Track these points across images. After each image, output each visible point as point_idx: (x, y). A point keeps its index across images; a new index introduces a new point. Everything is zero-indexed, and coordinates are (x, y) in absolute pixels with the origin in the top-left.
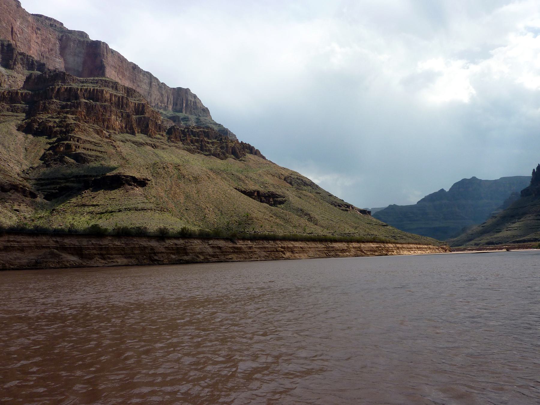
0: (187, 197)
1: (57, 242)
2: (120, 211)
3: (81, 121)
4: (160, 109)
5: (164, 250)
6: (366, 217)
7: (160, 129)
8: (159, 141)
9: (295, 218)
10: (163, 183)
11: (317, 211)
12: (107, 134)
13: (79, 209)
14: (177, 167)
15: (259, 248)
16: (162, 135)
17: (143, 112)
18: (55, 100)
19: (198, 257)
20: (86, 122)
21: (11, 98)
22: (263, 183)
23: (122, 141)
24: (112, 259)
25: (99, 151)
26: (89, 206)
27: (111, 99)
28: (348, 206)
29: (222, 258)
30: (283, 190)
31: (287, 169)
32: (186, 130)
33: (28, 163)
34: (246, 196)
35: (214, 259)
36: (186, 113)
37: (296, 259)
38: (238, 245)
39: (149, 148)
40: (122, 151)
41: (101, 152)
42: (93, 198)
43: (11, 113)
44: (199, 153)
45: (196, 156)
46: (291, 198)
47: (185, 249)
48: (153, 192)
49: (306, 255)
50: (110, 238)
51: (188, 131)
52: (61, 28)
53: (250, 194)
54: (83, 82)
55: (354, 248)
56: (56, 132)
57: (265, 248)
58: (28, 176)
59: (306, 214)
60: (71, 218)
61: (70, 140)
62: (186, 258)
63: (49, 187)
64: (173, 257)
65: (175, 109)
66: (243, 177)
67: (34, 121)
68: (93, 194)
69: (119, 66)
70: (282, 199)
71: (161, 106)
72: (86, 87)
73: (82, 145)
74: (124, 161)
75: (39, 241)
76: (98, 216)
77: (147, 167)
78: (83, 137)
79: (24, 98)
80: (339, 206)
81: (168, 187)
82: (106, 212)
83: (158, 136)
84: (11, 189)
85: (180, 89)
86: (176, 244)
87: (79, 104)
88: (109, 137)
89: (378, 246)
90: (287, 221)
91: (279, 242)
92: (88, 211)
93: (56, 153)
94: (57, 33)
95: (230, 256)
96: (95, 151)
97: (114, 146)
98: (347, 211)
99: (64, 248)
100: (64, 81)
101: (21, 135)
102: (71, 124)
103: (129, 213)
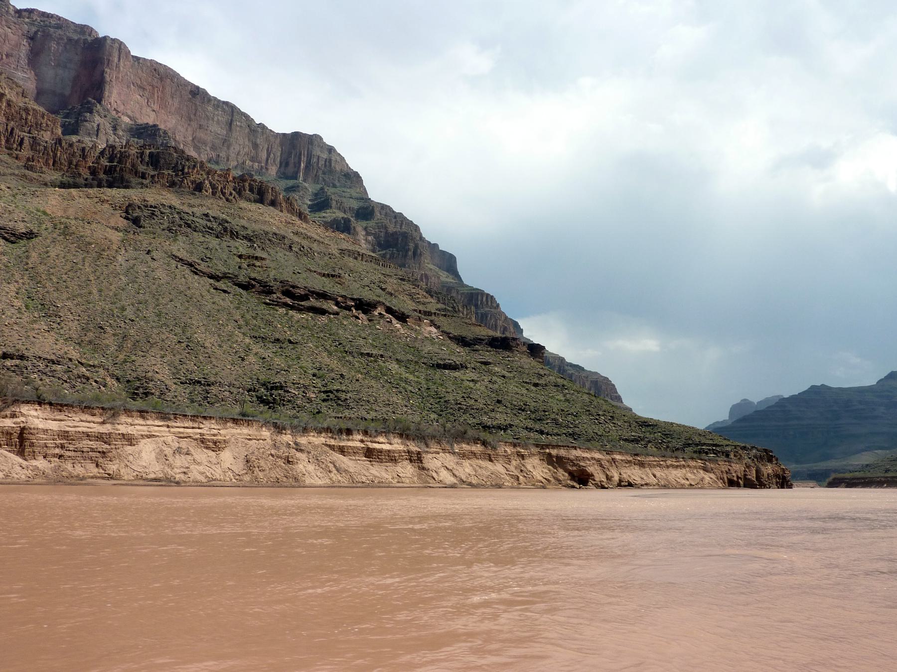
36: (305, 180)
65: (284, 173)
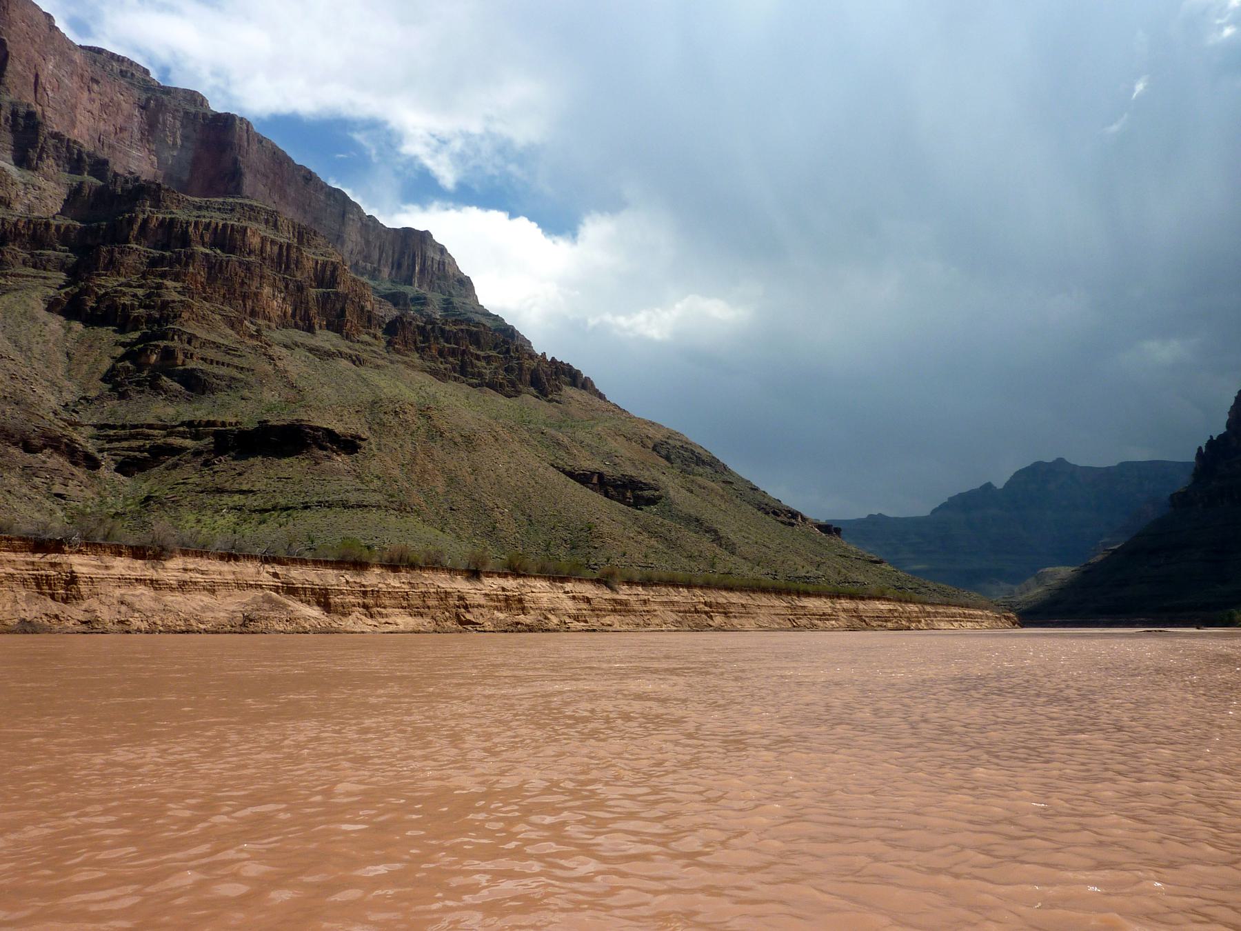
0: (452, 481)
1: (275, 575)
3: (196, 296)
4: (362, 274)
5: (483, 601)
6: (834, 540)
7: (369, 321)
8: (368, 348)
9: (690, 538)
10: (397, 446)
11: (732, 522)
12: (253, 328)
13: (208, 500)
14: (424, 412)
15: (662, 603)
16: (375, 337)
17: (333, 282)
18: (135, 246)
19: (546, 618)
20: (205, 299)
22: (609, 455)
23: (286, 346)
24: (387, 616)
25: (237, 367)
26: (232, 492)
27: (262, 250)
28: (794, 515)
29: (593, 621)
30: (656, 473)
31: (660, 426)
33: (74, 388)
34: (578, 485)
35: (580, 625)
36: (420, 286)
37: (734, 630)
38: (621, 597)
39: (344, 363)
40: (288, 369)
41: (242, 368)
42: (240, 474)
43: (31, 271)
44: (456, 379)
45: (451, 386)
46: (672, 493)
47: (520, 601)
48: (375, 466)
49: (753, 622)
50: (378, 571)
51: (433, 330)
53: (583, 478)
54: (200, 208)
55: (844, 610)
56: (137, 319)
57: (672, 603)
58: (76, 417)
59: (709, 530)
60: (192, 518)
62: (522, 618)
63: (125, 444)
64: (501, 616)
66: (566, 441)
67: (86, 291)
68: (241, 465)
69: (275, 174)
70: (652, 492)
71: (365, 268)
72: (208, 220)
73: (198, 352)
74: (294, 391)
75: (241, 573)
76: (256, 516)
77: (358, 409)
78: (202, 334)
79: (64, 236)
80: (774, 513)
81: (408, 457)
82: (274, 509)
83: (366, 338)
86: (504, 589)
87: (191, 256)
89: (891, 607)
90: (672, 544)
91: (698, 592)
92: (231, 504)
93: (140, 369)
94: (136, 92)
95: (607, 620)
96: (228, 365)
97: (271, 358)
98: (792, 525)
99: (291, 590)
100: (157, 203)
101: (55, 323)
102: (174, 302)
103: (331, 513)
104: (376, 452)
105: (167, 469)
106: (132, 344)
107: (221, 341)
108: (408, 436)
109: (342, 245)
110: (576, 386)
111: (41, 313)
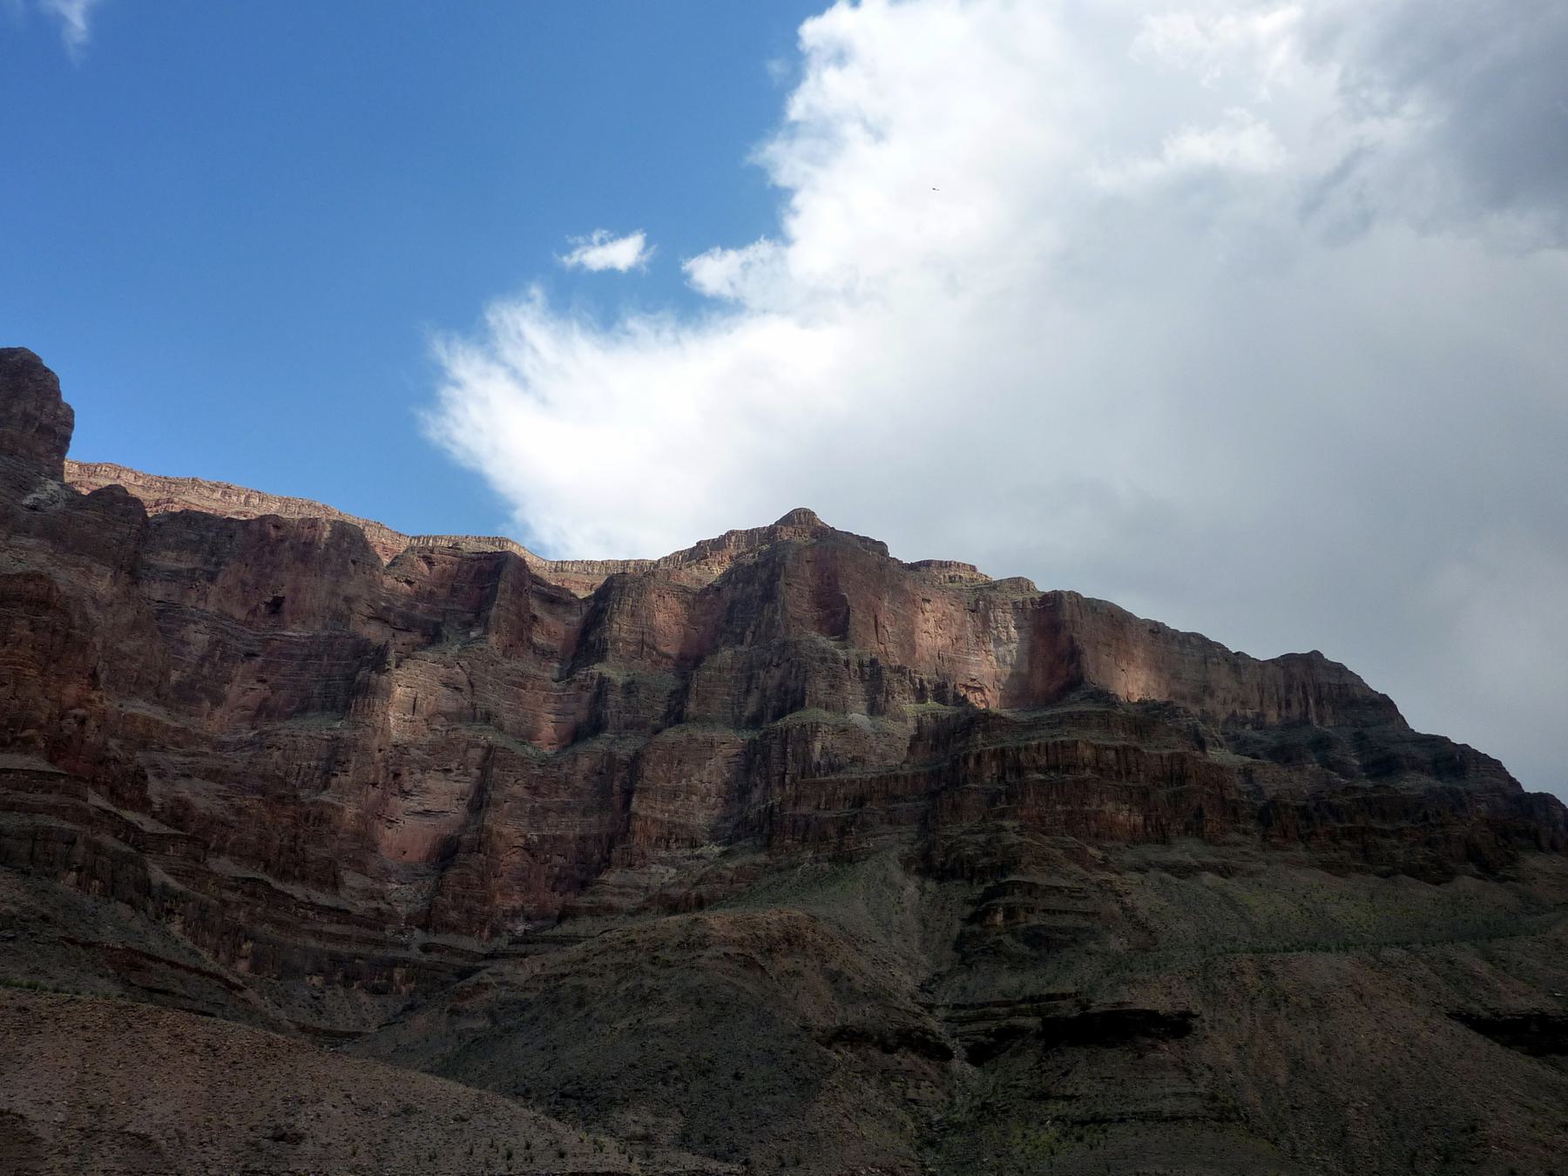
2: (1122, 1120)
8: (1237, 850)
12: (1099, 854)
16: (1245, 833)
17: (1182, 778)
20: (1044, 833)
21: (886, 789)
23: (1139, 870)
26: (1057, 1098)
32: (1313, 804)
39: (1208, 878)
40: (1139, 903)
44: (1358, 869)
52: (972, 580)
58: (928, 999)
60: (1019, 1132)
61: (1013, 893)
63: (974, 1027)
71: (1245, 717)
76: (1076, 1129)
78: (1041, 880)
81: (1245, 1035)
82: (1093, 1120)
83: (1236, 837)
84: (899, 1045)
85: (1289, 660)
88: (1105, 865)
104: (1208, 1031)
105: (1012, 1055)
106: (981, 901)
107: (1063, 883)
108: (1246, 1005)
109: (1212, 695)
110: (1541, 849)
111: (897, 875)
